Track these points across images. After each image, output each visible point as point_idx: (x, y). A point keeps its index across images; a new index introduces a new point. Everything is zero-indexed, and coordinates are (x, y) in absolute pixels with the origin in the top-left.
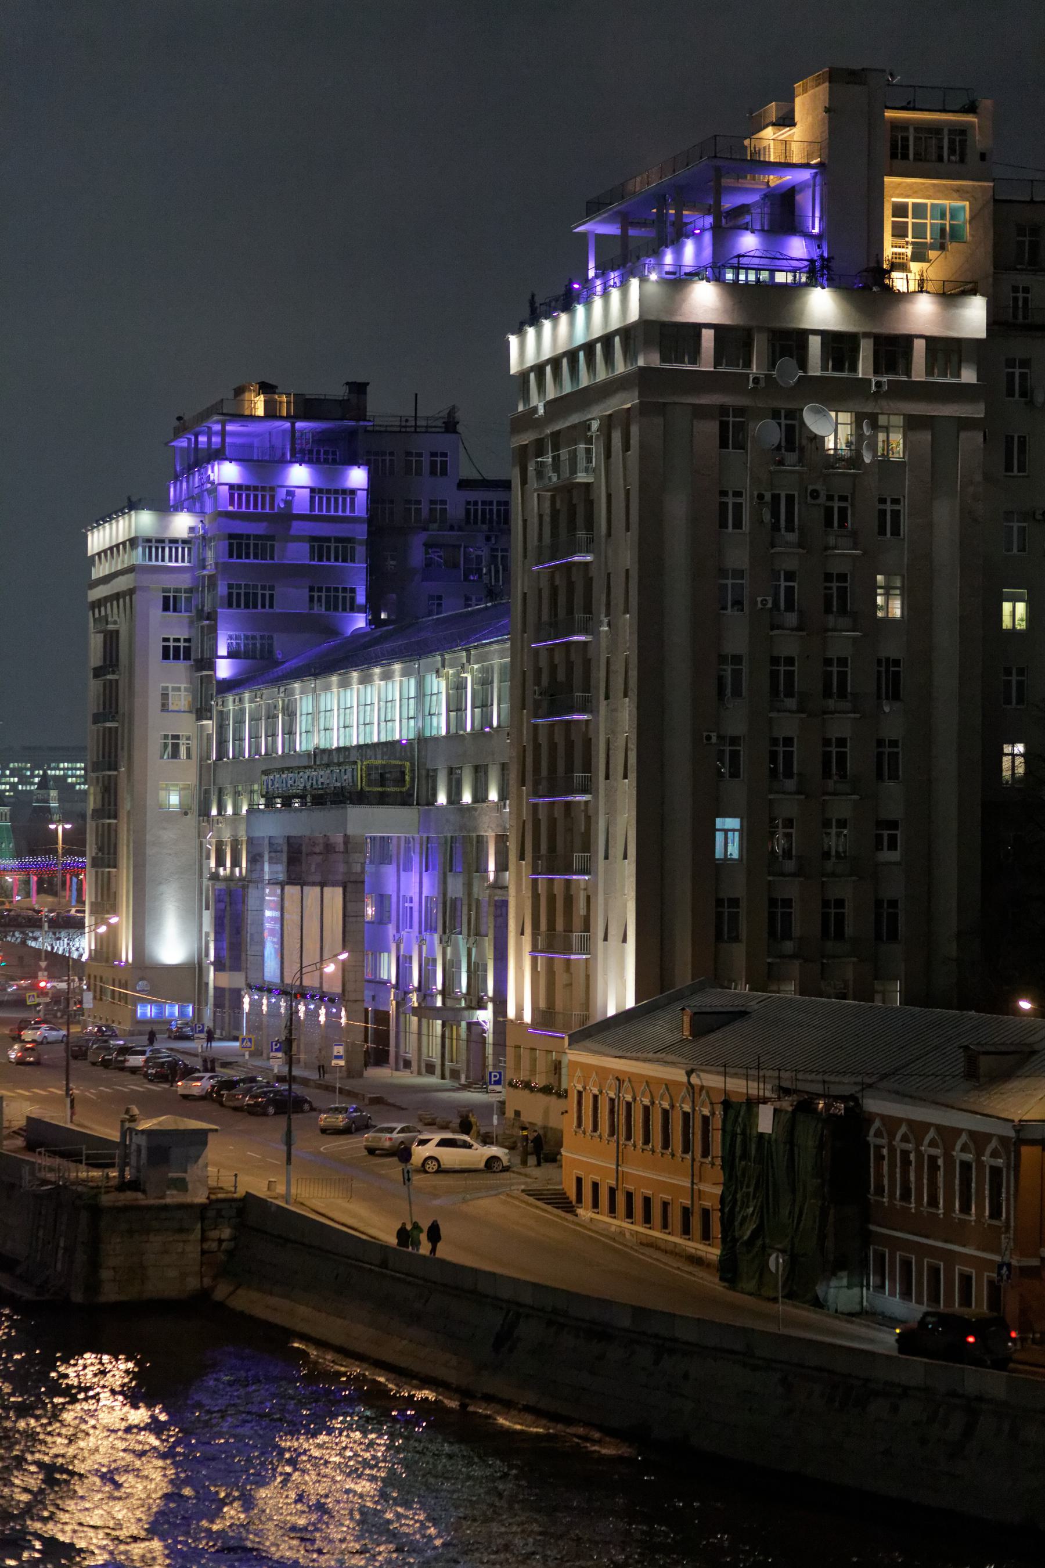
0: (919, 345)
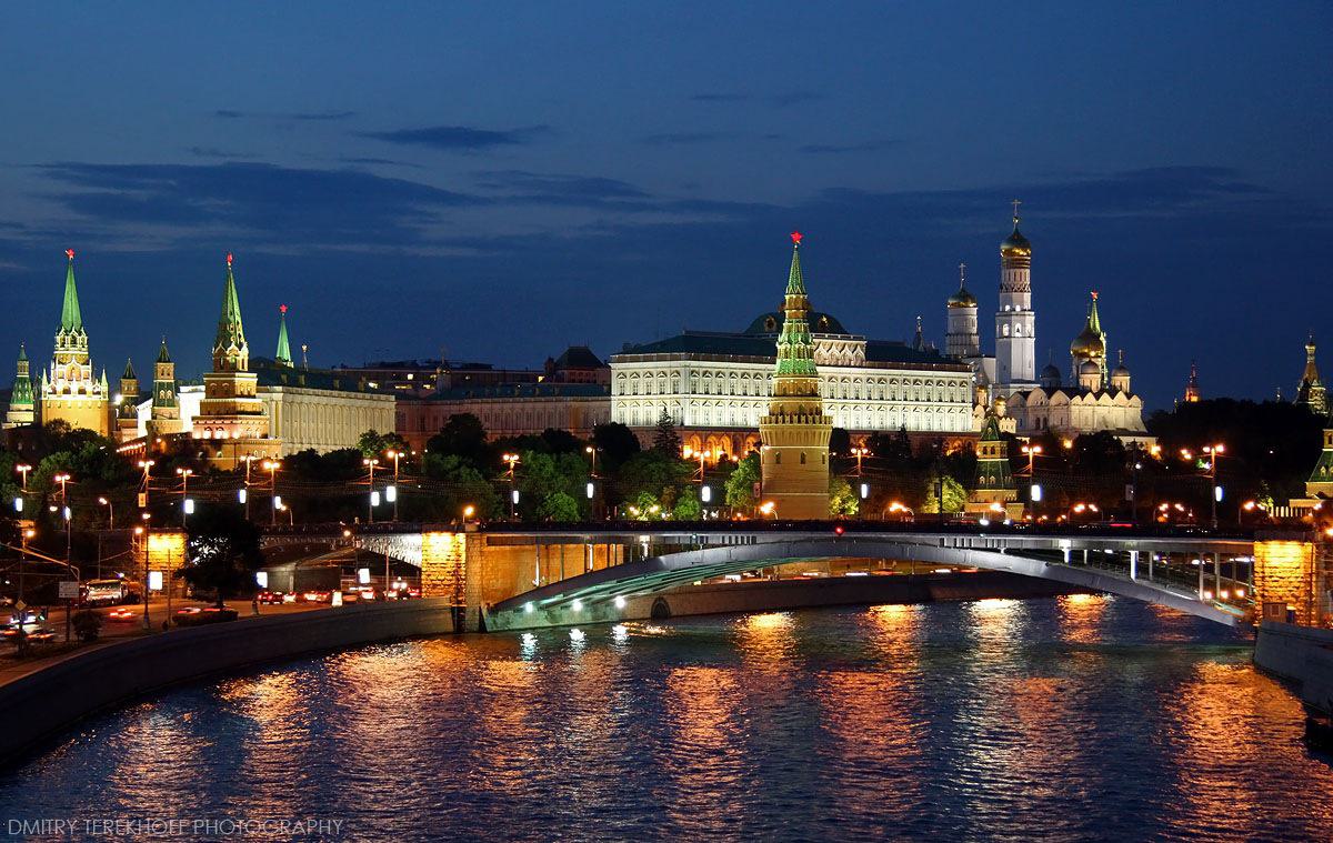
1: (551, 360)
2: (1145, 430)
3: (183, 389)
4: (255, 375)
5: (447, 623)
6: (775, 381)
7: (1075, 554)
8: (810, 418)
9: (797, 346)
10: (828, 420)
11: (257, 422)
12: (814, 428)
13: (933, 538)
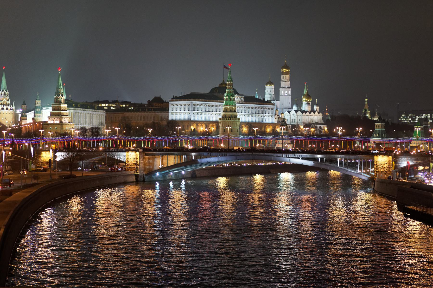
1: (149, 100)
2: (323, 123)
3: (43, 108)
4: (67, 104)
5: (134, 179)
6: (224, 107)
7: (322, 159)
8: (234, 118)
9: (230, 97)
10: (239, 119)
11: (67, 118)
12: (235, 121)
13: (280, 155)
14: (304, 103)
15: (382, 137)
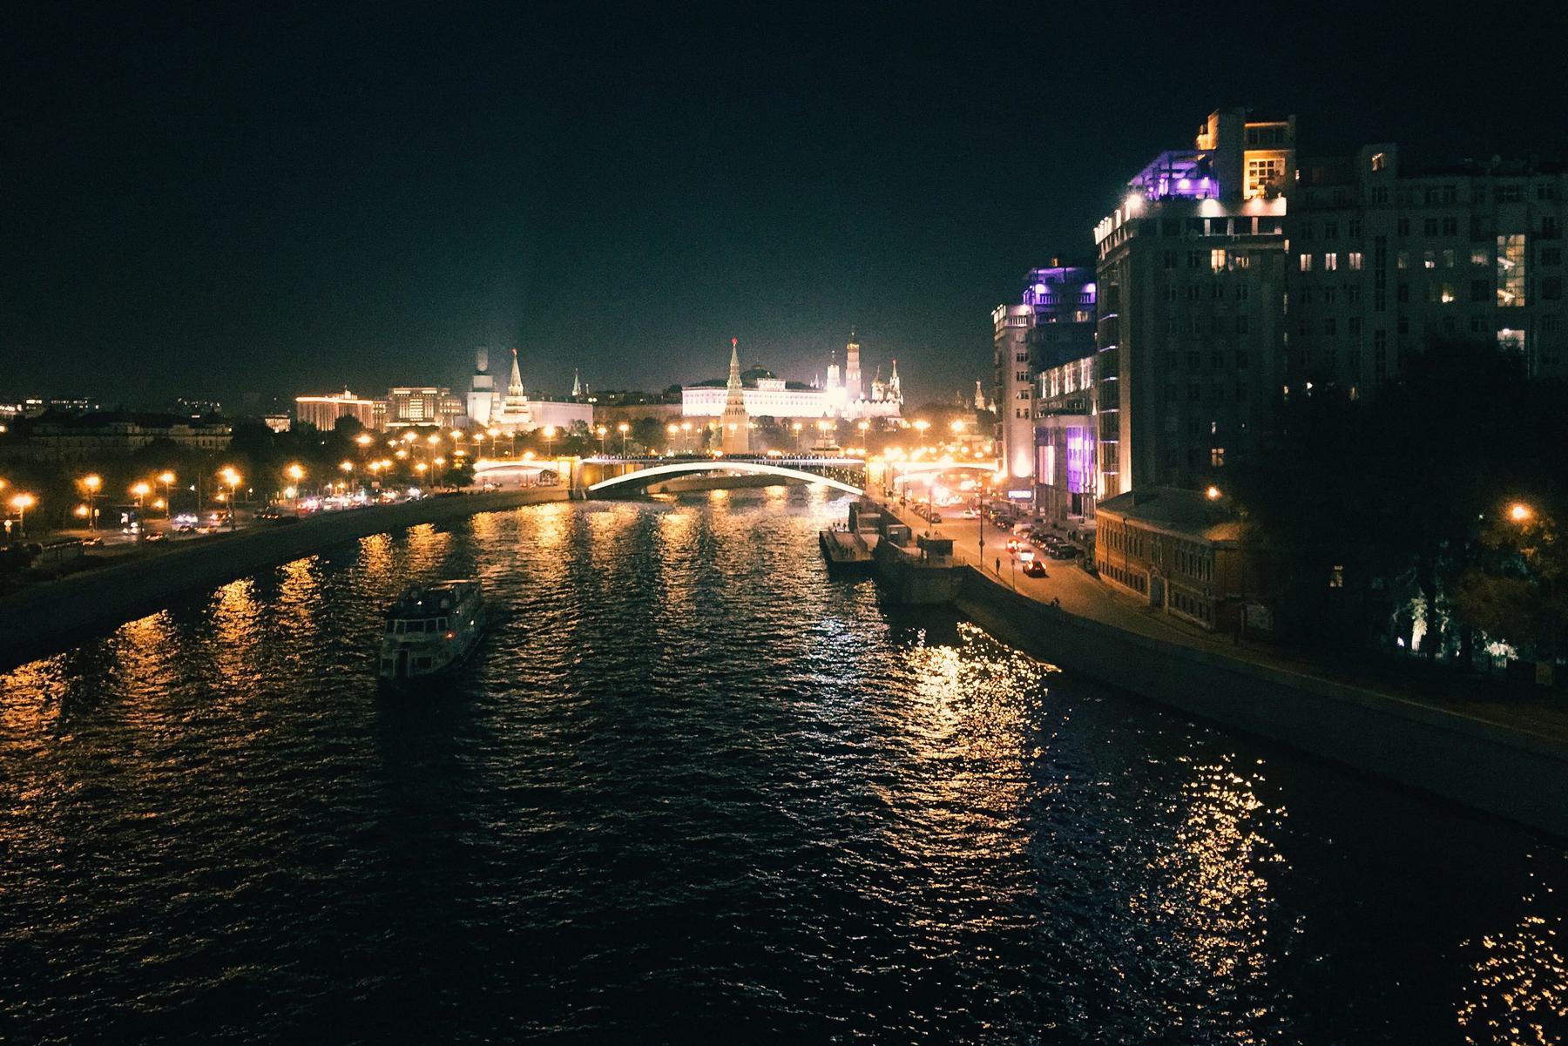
0: (1255, 221)
6: (727, 398)
14: (874, 389)
15: (973, 434)
